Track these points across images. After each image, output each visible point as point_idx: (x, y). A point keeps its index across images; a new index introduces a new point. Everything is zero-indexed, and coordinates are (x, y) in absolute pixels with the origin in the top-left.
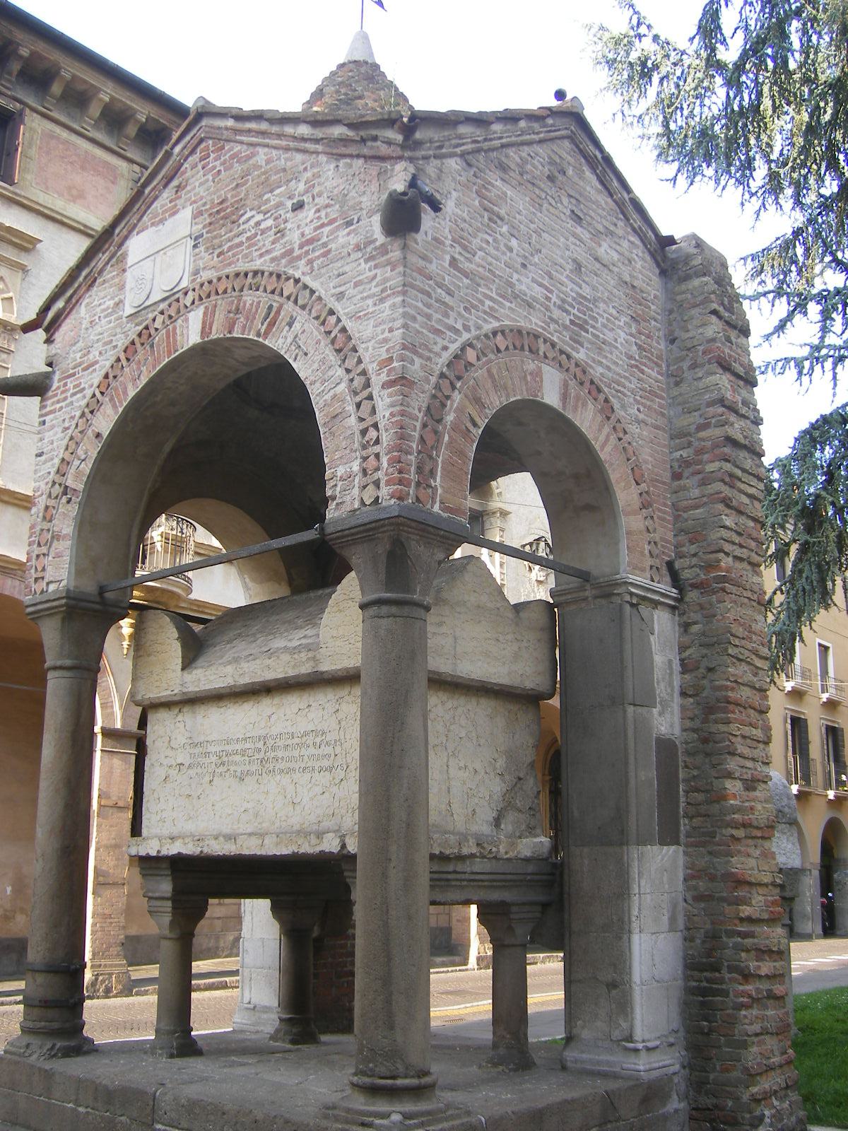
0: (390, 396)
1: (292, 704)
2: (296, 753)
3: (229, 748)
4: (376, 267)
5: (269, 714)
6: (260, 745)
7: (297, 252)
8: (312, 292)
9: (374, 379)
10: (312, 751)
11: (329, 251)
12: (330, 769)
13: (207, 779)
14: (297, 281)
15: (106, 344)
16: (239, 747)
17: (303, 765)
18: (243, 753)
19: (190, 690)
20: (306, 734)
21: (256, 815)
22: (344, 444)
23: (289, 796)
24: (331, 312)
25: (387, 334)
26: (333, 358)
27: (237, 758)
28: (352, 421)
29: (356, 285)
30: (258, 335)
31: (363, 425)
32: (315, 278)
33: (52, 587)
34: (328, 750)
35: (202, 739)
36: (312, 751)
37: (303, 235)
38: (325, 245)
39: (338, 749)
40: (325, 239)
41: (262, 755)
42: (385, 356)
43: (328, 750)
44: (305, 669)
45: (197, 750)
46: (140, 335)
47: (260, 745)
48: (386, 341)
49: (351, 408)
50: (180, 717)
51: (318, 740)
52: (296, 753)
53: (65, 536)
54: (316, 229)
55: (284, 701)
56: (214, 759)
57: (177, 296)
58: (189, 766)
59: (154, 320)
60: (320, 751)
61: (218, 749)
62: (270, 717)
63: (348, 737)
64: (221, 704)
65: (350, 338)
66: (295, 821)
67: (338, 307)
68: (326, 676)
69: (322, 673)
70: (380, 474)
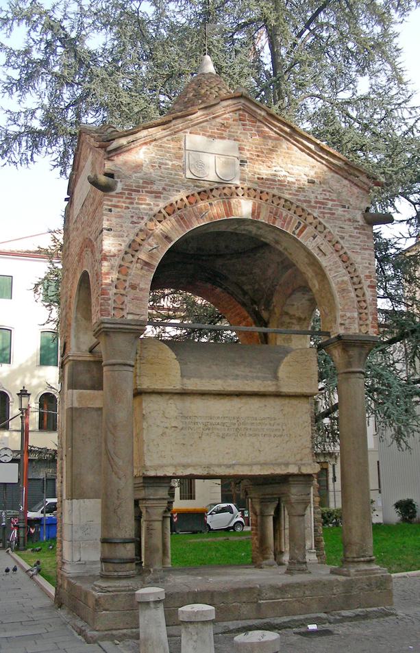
0: (371, 291)
1: (255, 403)
2: (259, 427)
3: (213, 421)
4: (360, 233)
5: (240, 406)
6: (235, 421)
7: (313, 204)
8: (325, 228)
9: (363, 281)
10: (268, 427)
11: (334, 214)
12: (281, 436)
13: (196, 436)
14: (315, 218)
15: (166, 185)
16: (219, 421)
17: (264, 433)
18: (223, 424)
19: (189, 388)
20: (264, 419)
21: (235, 455)
22: (349, 304)
23: (256, 447)
24: (337, 242)
25: (367, 265)
26: (340, 263)
27: (218, 427)
28: (353, 294)
29: (350, 236)
30: (294, 233)
31: (359, 299)
32: (327, 222)
33: (130, 317)
34: (279, 427)
35: (190, 414)
36: (268, 427)
37: (316, 197)
38: (330, 209)
39: (284, 427)
40: (329, 206)
41: (236, 426)
42: (368, 274)
43: (279, 427)
44: (272, 389)
45: (187, 421)
46: (199, 193)
47: (235, 421)
48: (368, 268)
49: (351, 288)
50: (171, 401)
51: (272, 422)
52: (259, 427)
53: (141, 290)
54: (324, 199)
55: (250, 402)
56: (202, 426)
57: (230, 185)
58: (182, 429)
59: (212, 190)
60: (274, 428)
61: (204, 421)
62: (240, 408)
63: (289, 422)
64: (203, 398)
65: (349, 258)
66: (262, 459)
67: (341, 241)
68: (282, 394)
69: (281, 392)
70: (368, 322)
